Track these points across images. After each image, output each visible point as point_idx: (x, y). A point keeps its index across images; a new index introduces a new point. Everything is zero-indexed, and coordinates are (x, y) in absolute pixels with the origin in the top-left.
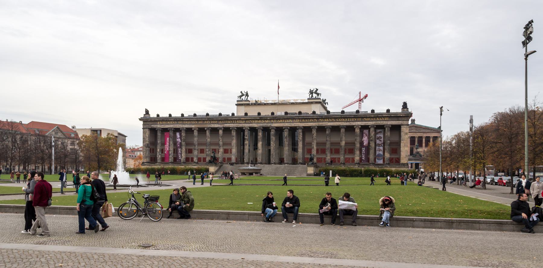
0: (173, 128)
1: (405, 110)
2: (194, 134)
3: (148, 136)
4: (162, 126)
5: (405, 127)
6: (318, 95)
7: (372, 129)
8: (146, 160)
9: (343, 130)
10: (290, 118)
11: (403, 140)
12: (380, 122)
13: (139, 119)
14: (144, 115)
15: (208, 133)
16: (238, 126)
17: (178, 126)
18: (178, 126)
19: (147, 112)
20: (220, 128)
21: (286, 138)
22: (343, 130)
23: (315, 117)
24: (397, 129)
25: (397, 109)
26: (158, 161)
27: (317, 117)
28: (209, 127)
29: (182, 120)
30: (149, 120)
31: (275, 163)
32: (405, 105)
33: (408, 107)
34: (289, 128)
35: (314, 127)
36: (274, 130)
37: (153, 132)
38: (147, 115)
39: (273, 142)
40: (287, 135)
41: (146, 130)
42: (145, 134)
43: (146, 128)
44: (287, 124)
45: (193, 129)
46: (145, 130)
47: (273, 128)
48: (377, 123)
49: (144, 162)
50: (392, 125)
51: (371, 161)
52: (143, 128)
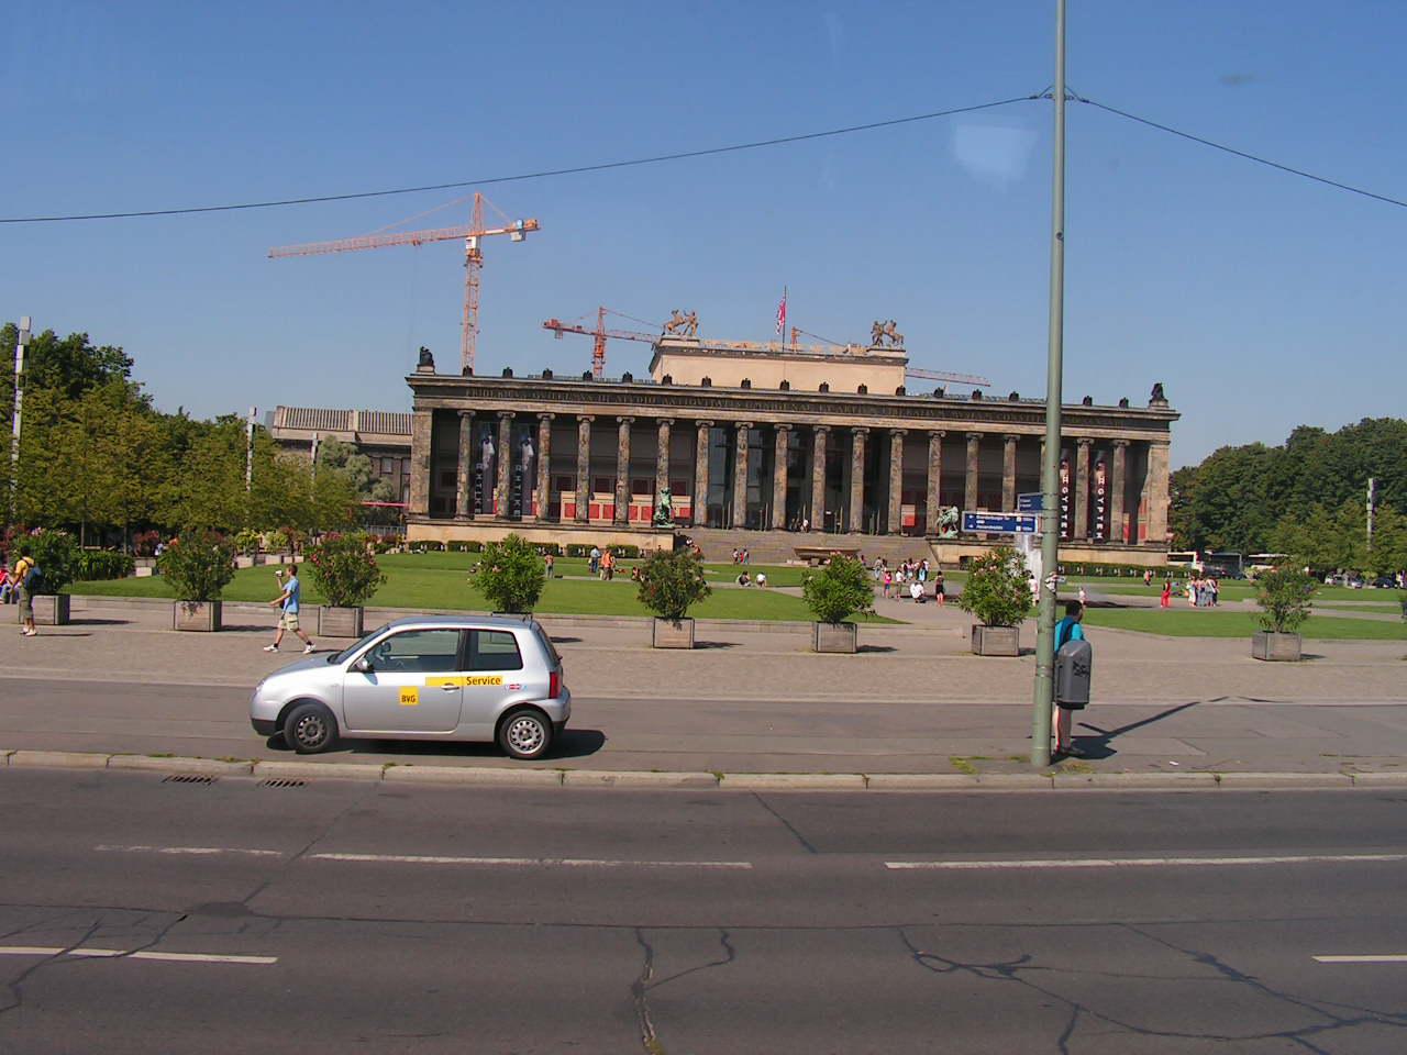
0: (516, 412)
1: (1161, 404)
2: (581, 433)
3: (430, 431)
4: (481, 405)
5: (1163, 446)
6: (894, 340)
7: (1083, 452)
8: (421, 505)
9: (1009, 447)
10: (875, 403)
11: (1156, 482)
12: (1102, 431)
13: (407, 379)
14: (418, 366)
15: (624, 431)
16: (721, 418)
17: (532, 407)
18: (532, 407)
19: (426, 358)
20: (666, 421)
21: (859, 457)
22: (1009, 447)
23: (943, 406)
24: (1138, 450)
25: (1140, 401)
26: (462, 513)
27: (946, 407)
28: (629, 414)
29: (547, 388)
30: (440, 384)
31: (778, 528)
32: (1158, 389)
33: (1166, 396)
34: (868, 430)
35: (937, 433)
36: (824, 435)
37: (444, 420)
38: (431, 369)
39: (823, 469)
40: (863, 452)
41: (426, 413)
42: (422, 425)
43: (426, 409)
44: (863, 419)
45: (579, 419)
46: (420, 413)
47: (822, 428)
48: (1096, 433)
49: (414, 514)
50: (1130, 440)
51: (1080, 532)
52: (414, 409)
